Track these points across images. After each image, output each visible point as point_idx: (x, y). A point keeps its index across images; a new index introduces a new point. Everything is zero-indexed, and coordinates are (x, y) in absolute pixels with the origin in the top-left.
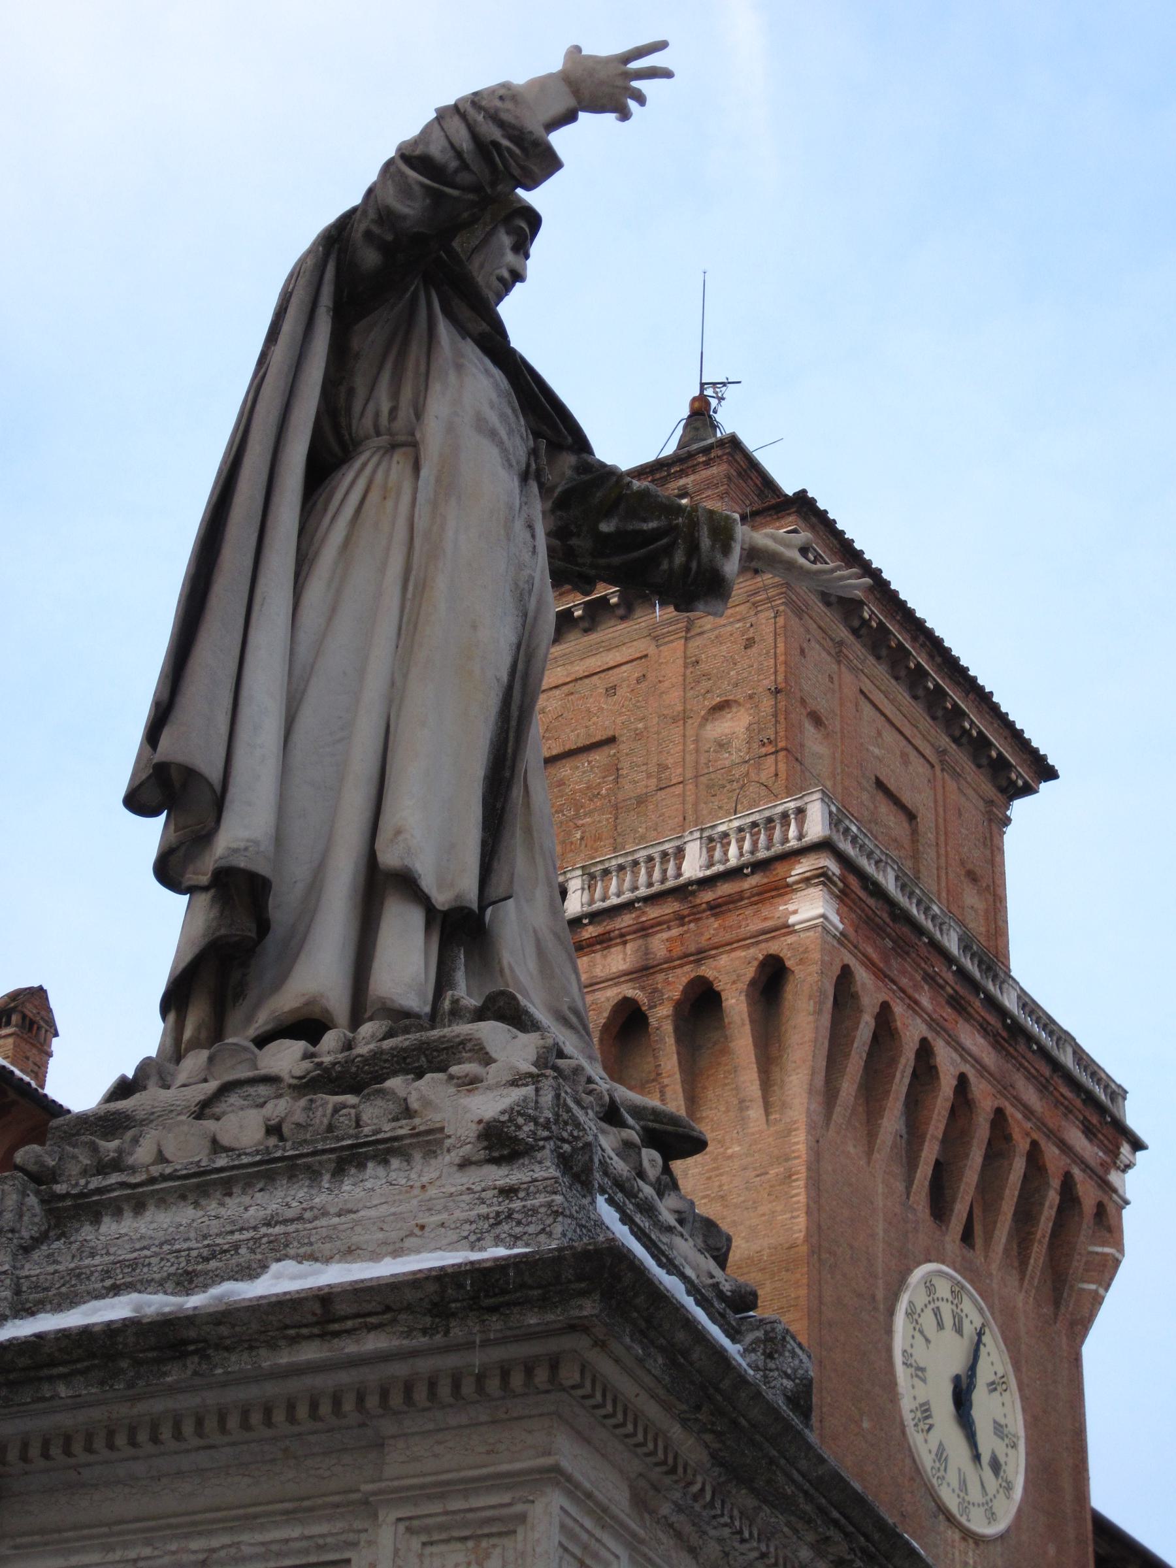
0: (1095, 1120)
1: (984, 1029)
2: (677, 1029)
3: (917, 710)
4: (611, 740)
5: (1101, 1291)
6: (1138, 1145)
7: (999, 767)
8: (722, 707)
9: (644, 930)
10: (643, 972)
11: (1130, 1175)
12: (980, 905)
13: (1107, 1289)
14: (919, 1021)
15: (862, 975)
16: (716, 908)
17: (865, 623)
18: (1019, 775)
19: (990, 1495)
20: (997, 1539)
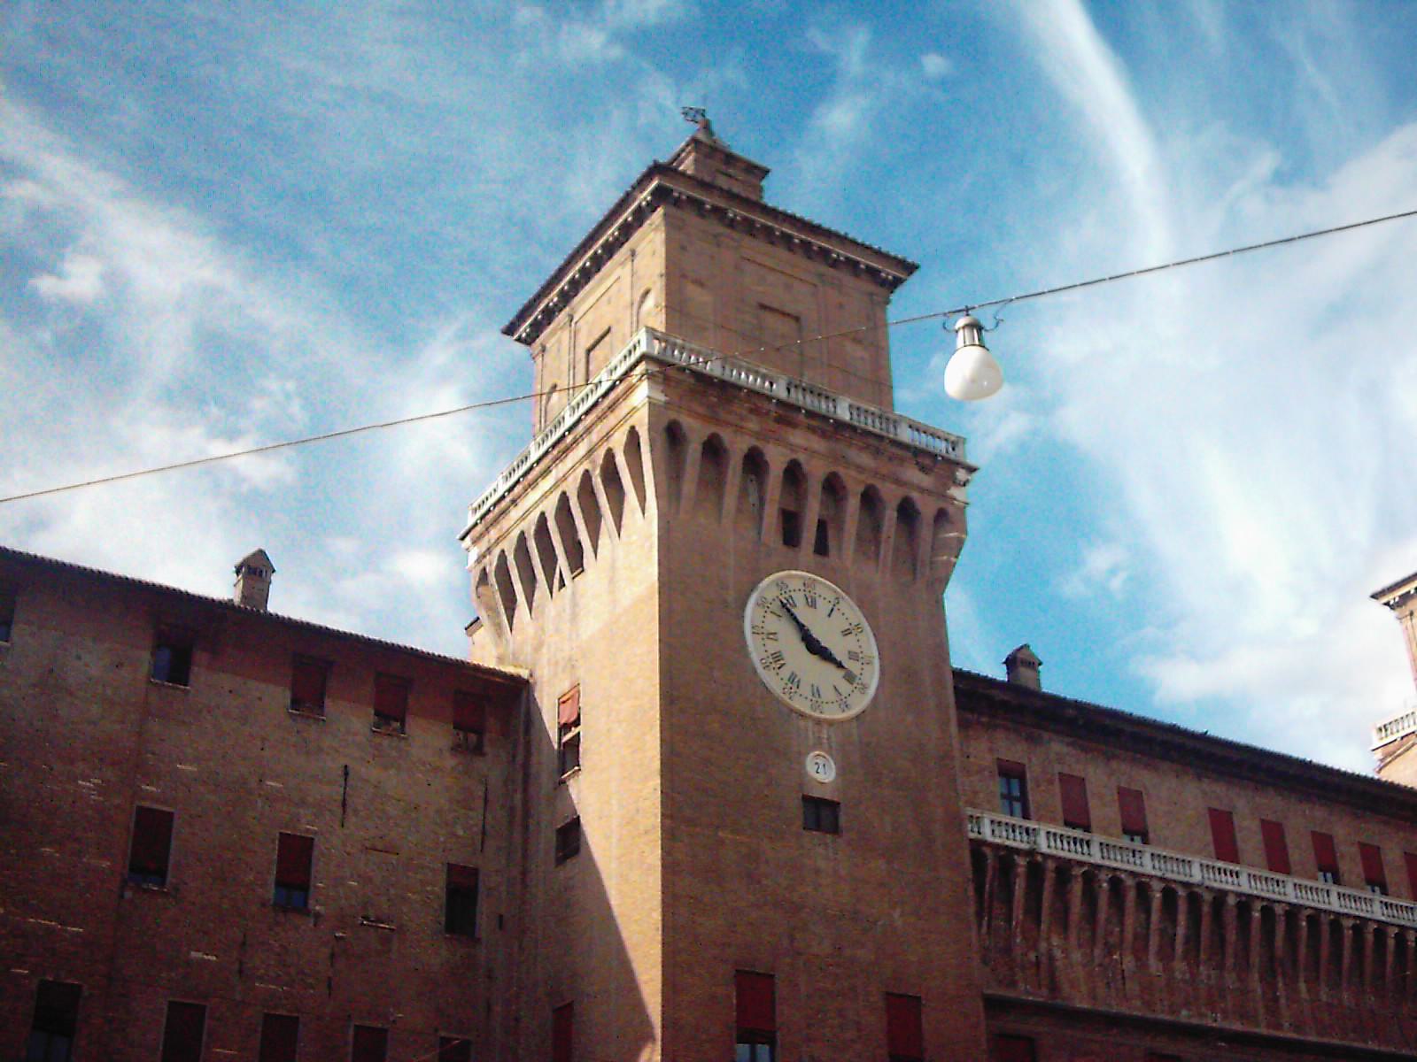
0: (927, 462)
1: (812, 429)
2: (604, 481)
3: (800, 260)
4: (609, 330)
5: (953, 559)
6: (972, 470)
7: (873, 273)
8: (647, 292)
9: (588, 430)
10: (590, 452)
11: (969, 487)
12: (866, 355)
13: (957, 557)
14: (747, 437)
15: (688, 422)
16: (611, 408)
17: (733, 220)
18: (888, 274)
19: (845, 694)
20: (853, 719)
